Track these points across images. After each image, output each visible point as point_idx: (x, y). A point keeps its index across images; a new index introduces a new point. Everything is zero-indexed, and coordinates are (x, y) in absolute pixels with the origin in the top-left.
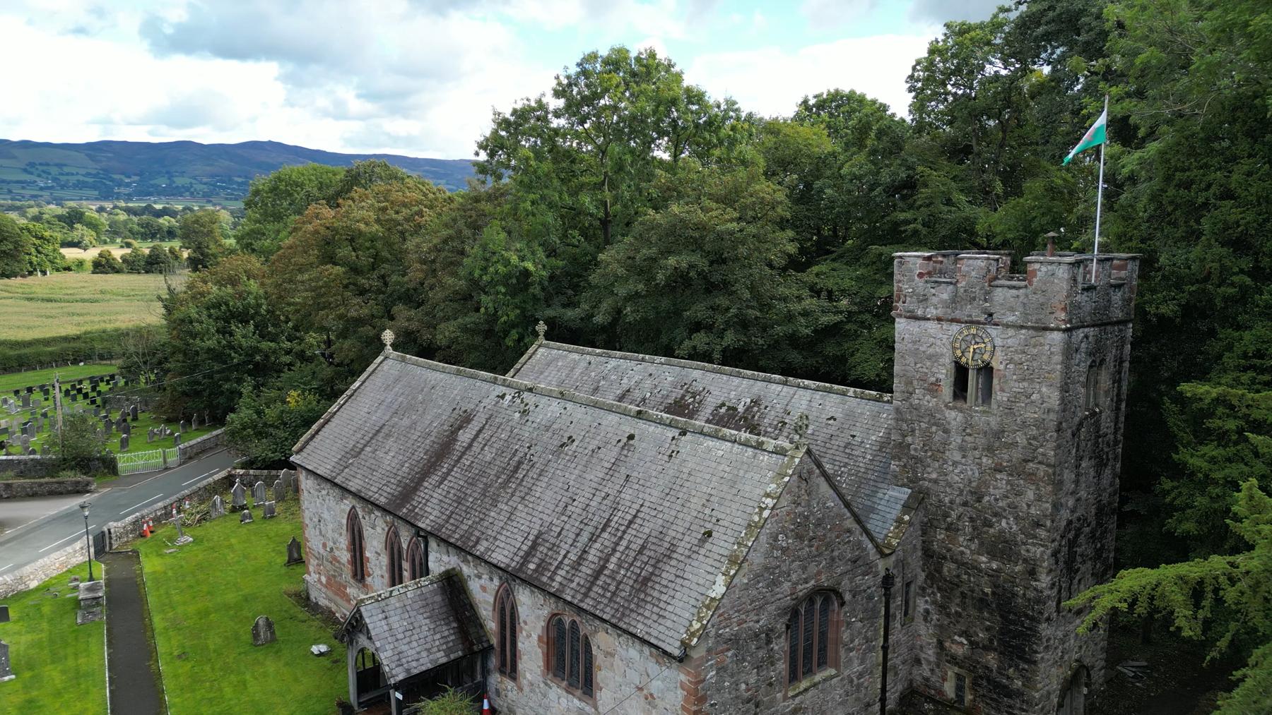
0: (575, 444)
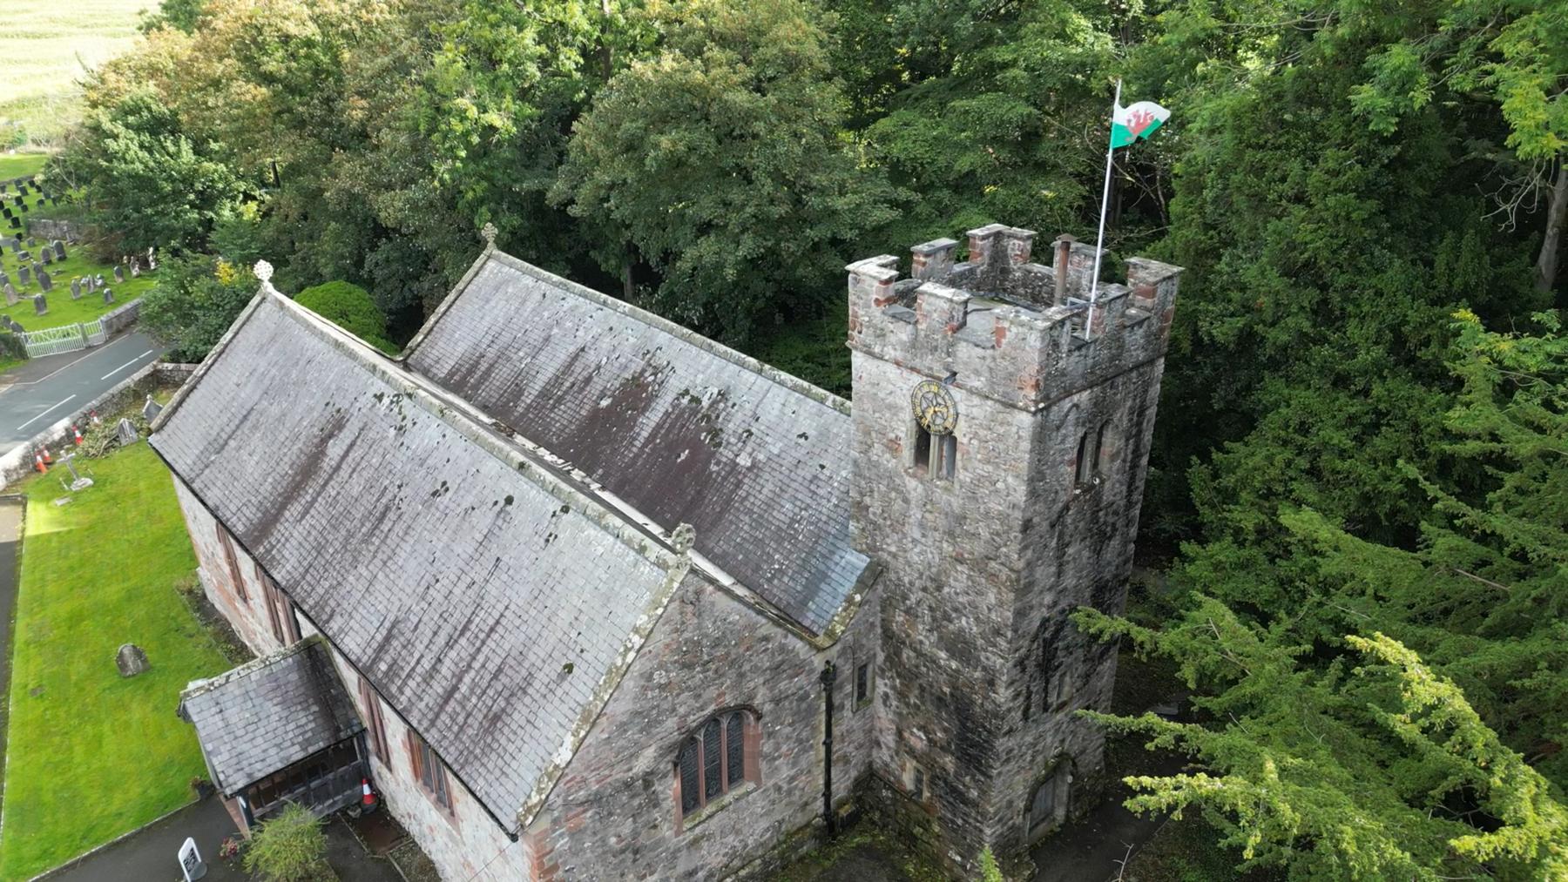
0: (449, 494)
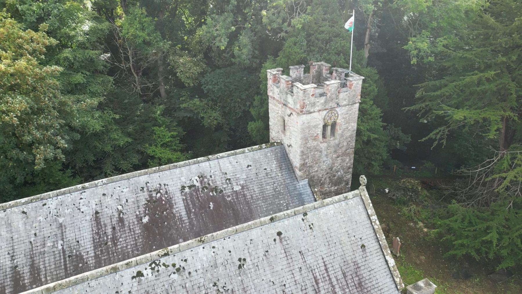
0: (248, 260)
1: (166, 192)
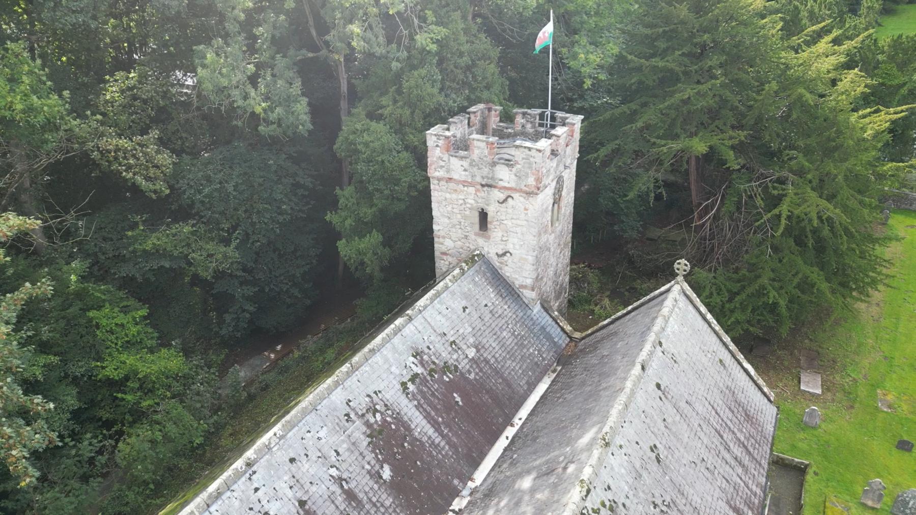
0: (658, 445)
1: (386, 405)
